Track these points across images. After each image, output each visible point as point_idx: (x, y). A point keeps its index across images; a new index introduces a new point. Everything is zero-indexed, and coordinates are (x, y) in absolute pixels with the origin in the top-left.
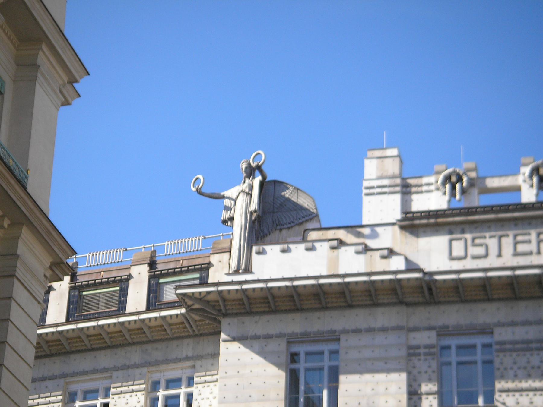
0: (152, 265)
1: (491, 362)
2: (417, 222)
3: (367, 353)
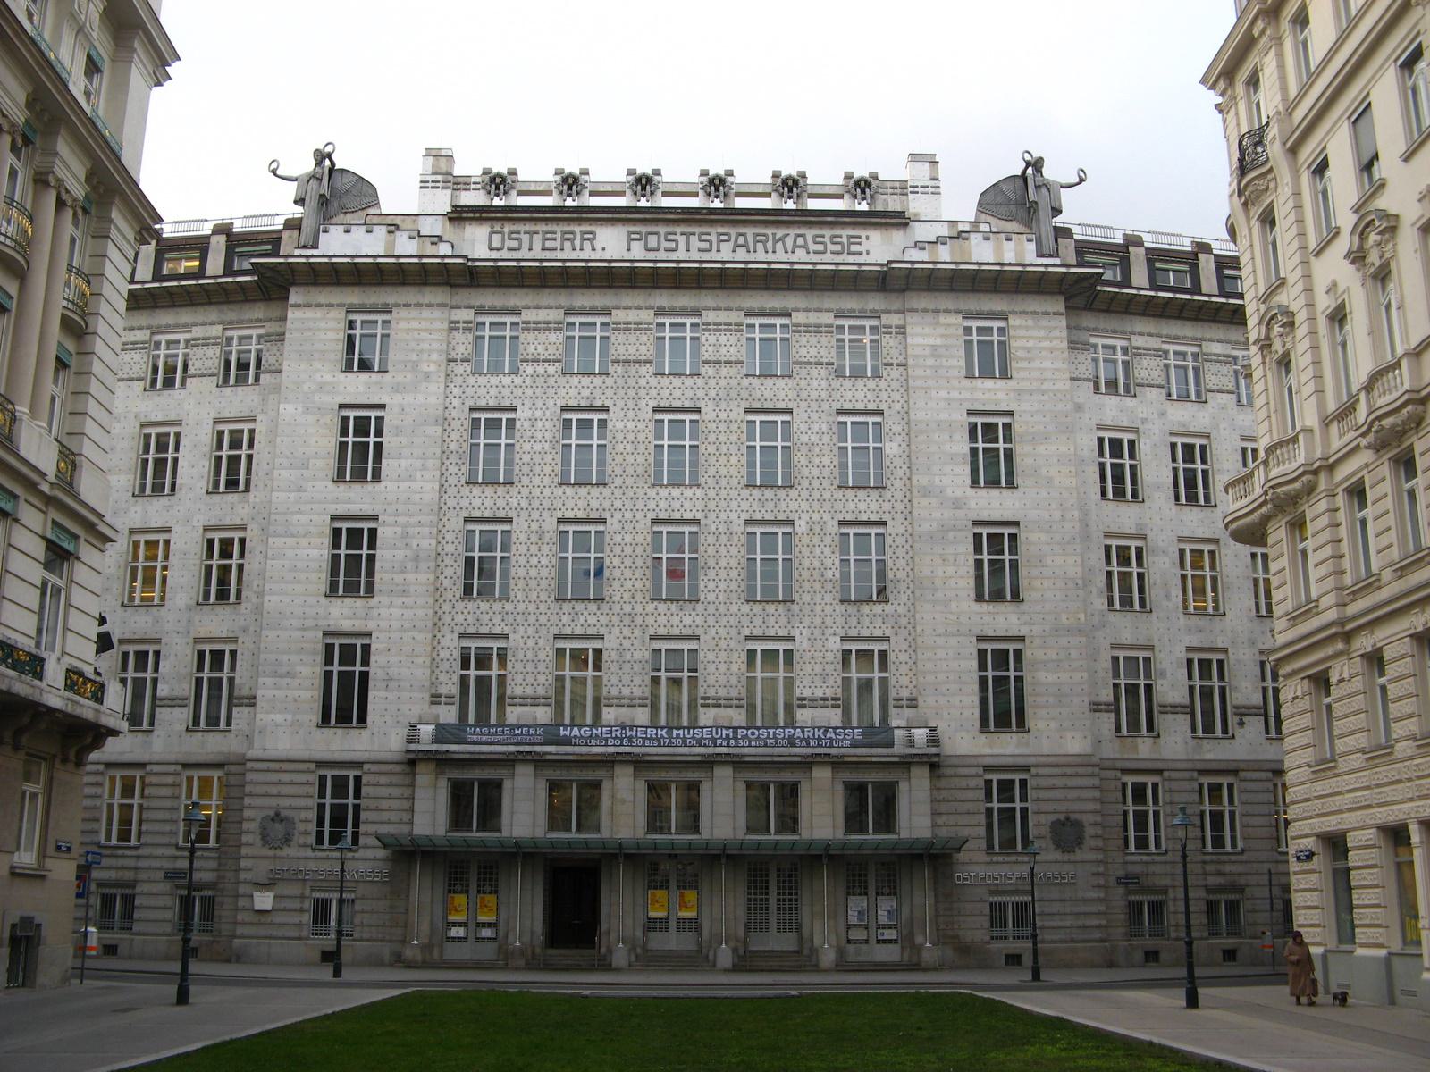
0: (228, 235)
1: (517, 337)
2: (464, 215)
3: (414, 325)
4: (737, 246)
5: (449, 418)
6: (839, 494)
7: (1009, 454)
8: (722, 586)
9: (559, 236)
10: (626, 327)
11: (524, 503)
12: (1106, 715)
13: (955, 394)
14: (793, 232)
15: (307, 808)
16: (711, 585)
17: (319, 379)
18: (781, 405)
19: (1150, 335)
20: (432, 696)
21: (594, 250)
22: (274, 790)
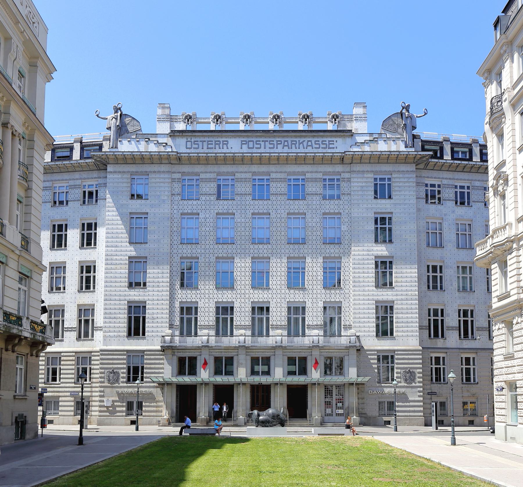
0: (81, 142)
3: (158, 180)
4: (284, 146)
5: (173, 218)
6: (323, 246)
7: (390, 230)
8: (279, 283)
9: (214, 143)
10: (241, 180)
11: (203, 251)
12: (425, 331)
13: (369, 206)
14: (306, 139)
15: (123, 368)
16: (274, 282)
17: (121, 202)
18: (301, 211)
19: (450, 179)
20: (170, 325)
21: (228, 148)
22: (111, 362)
